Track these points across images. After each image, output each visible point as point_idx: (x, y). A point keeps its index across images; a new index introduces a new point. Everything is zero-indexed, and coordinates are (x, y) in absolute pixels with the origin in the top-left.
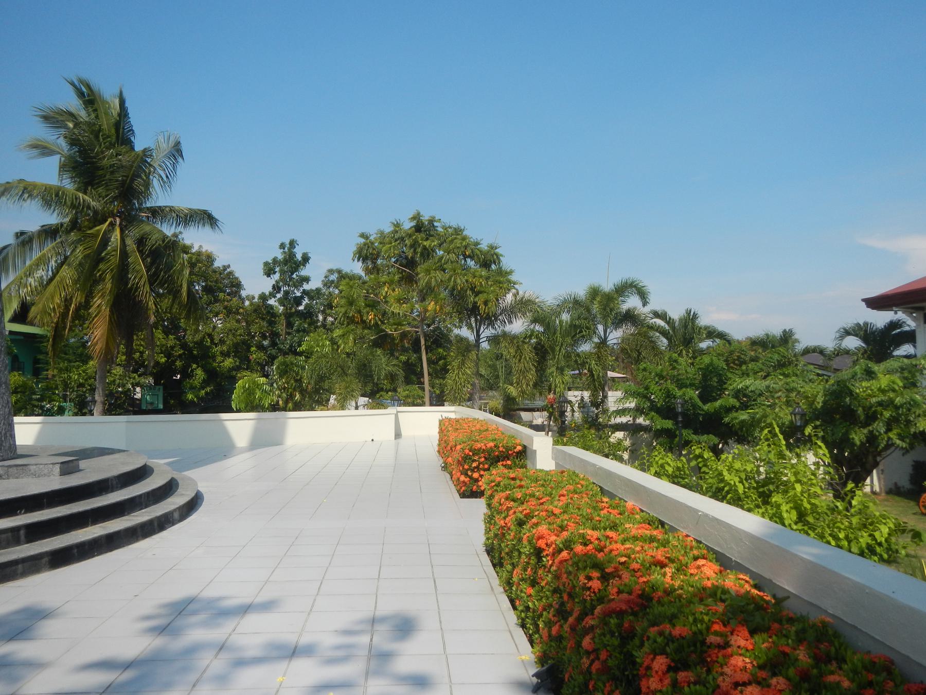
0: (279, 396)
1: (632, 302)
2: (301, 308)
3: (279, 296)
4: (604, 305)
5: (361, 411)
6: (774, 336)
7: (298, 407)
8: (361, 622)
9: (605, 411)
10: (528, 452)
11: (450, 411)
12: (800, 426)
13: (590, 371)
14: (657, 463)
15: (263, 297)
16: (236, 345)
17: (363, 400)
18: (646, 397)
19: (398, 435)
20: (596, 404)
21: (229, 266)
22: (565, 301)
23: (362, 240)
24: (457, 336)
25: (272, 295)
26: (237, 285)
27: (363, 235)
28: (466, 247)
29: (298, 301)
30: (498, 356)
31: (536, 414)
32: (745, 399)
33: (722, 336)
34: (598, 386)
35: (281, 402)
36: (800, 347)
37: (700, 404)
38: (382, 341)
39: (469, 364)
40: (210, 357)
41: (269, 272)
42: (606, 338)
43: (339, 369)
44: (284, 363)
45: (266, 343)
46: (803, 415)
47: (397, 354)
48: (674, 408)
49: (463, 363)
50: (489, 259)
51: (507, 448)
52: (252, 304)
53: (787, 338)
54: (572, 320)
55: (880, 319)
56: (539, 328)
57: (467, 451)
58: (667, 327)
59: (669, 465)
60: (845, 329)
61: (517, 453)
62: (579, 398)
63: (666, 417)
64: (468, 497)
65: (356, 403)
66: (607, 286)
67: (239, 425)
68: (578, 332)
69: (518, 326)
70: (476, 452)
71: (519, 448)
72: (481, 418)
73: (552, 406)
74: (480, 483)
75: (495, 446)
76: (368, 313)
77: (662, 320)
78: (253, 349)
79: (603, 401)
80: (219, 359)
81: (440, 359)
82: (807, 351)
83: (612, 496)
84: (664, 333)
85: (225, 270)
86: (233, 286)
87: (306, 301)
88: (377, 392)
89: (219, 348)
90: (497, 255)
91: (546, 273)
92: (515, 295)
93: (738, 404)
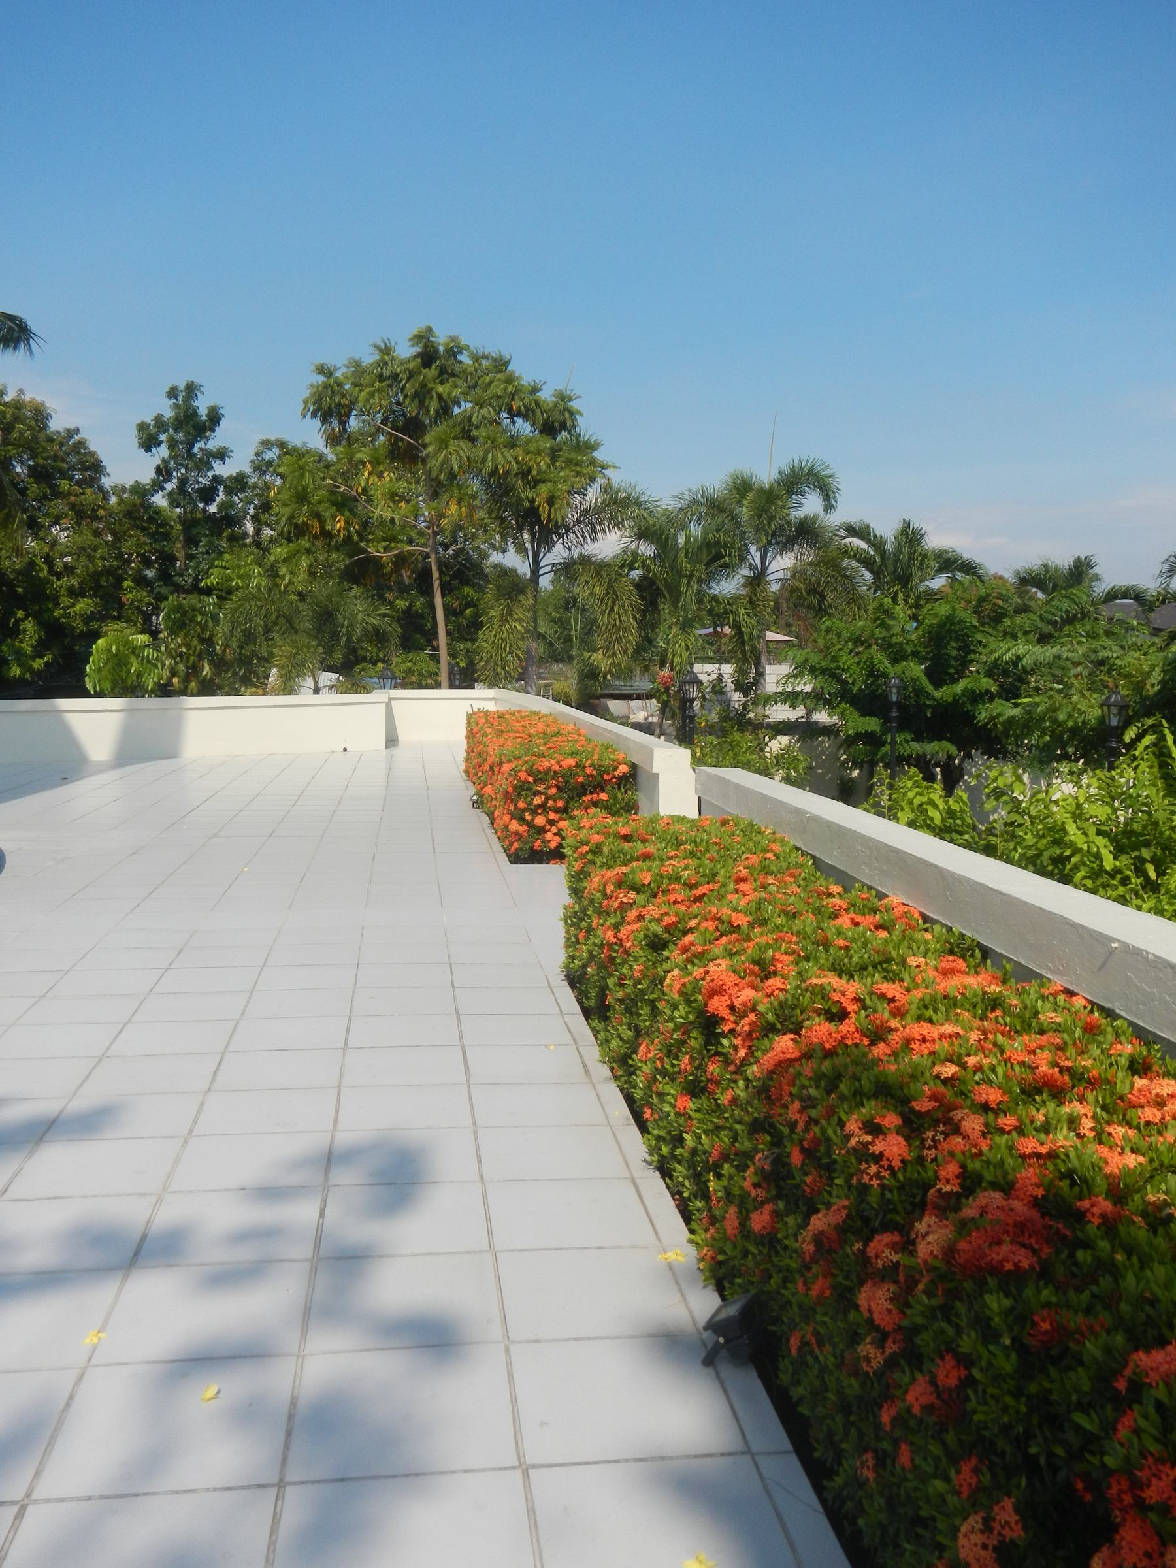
2: (213, 508)
3: (169, 486)
4: (761, 511)
5: (325, 697)
6: (1056, 569)
7: (207, 689)
8: (301, 1163)
10: (642, 779)
11: (485, 698)
12: (1117, 728)
13: (736, 626)
14: (911, 803)
15: (140, 491)
16: (95, 576)
17: (327, 678)
18: (832, 674)
19: (392, 741)
20: (740, 687)
21: (77, 431)
23: (321, 379)
24: (495, 566)
25: (157, 486)
26: (95, 467)
27: (321, 370)
28: (512, 396)
29: (208, 495)
30: (568, 603)
32: (1012, 681)
33: (968, 567)
34: (747, 656)
35: (175, 680)
36: (1101, 588)
37: (930, 688)
38: (362, 572)
39: (519, 613)
40: (48, 599)
41: (148, 442)
42: (764, 569)
43: (282, 621)
44: (179, 608)
45: (150, 574)
46: (1123, 708)
47: (389, 596)
48: (886, 697)
49: (510, 612)
50: (555, 422)
51: (601, 770)
52: (121, 501)
53: (1080, 571)
54: (705, 533)
56: (647, 549)
57: (523, 775)
59: (936, 806)
61: (620, 778)
62: (714, 676)
63: (865, 712)
64: (525, 861)
65: (316, 683)
66: (766, 475)
67: (94, 722)
68: (717, 556)
69: (609, 544)
70: (540, 776)
71: (623, 769)
72: (545, 711)
73: (667, 690)
74: (549, 836)
75: (577, 765)
78: (127, 584)
79: (756, 683)
80: (65, 601)
81: (468, 606)
82: (1112, 596)
83: (846, 881)
84: (867, 563)
86: (85, 469)
87: (221, 496)
88: (354, 663)
89: (64, 581)
90: (571, 413)
91: (662, 447)
92: (606, 489)
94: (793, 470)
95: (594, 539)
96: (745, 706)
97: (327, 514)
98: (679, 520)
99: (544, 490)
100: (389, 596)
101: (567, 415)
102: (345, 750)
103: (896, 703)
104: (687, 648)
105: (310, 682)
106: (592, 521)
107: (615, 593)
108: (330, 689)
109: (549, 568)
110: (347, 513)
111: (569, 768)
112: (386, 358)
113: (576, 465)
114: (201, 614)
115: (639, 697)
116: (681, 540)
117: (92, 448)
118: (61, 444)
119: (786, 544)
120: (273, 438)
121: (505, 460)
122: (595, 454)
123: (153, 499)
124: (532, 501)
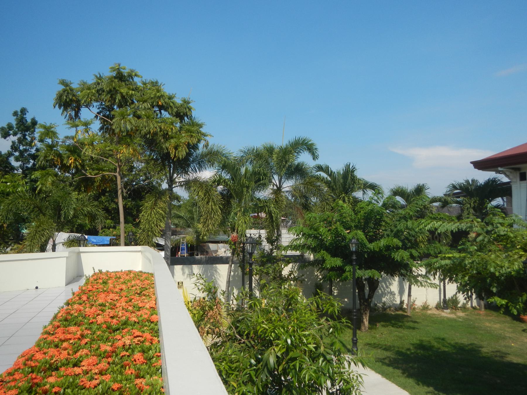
1: (304, 158)
9: (278, 248)
13: (270, 213)
28: (159, 98)
30: (194, 205)
31: (220, 245)
39: (161, 204)
42: (280, 186)
49: (155, 204)
50: (182, 113)
54: (254, 168)
55: (483, 177)
56: (226, 176)
58: (329, 179)
60: (453, 185)
62: (257, 236)
63: (334, 255)
68: (260, 179)
76: (68, 157)
77: (324, 172)
82: (434, 200)
91: (233, 129)
92: (206, 146)
93: (400, 244)
96: (272, 250)
98: (241, 161)
101: (187, 110)
102: (37, 288)
107: (209, 195)
113: (191, 132)
116: (243, 170)
120: (70, 135)
121: (153, 127)
122: (201, 129)
124: (167, 149)
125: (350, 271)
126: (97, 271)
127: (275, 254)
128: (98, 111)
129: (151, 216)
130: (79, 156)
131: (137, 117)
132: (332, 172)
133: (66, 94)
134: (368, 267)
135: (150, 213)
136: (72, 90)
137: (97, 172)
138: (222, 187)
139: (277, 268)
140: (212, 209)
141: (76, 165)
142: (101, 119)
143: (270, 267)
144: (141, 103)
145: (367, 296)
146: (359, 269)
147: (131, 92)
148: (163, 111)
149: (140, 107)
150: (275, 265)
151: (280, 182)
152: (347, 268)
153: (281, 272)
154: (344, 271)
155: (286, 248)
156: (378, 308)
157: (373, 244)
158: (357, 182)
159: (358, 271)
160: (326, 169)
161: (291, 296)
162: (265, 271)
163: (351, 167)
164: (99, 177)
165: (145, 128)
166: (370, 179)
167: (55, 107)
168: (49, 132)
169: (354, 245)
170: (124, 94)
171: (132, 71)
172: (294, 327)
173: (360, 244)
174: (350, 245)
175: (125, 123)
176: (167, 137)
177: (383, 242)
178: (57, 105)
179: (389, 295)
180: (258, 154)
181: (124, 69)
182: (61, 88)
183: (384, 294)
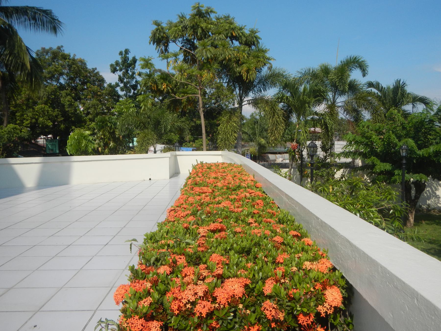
0: (99, 144)
1: (355, 75)
5: (159, 154)
9: (332, 155)
17: (159, 147)
18: (366, 145)
22: (305, 75)
23: (155, 27)
26: (102, 80)
30: (255, 123)
31: (278, 156)
35: (100, 149)
42: (334, 101)
43: (142, 124)
47: (194, 120)
49: (230, 118)
50: (251, 41)
58: (379, 94)
63: (383, 160)
65: (155, 149)
71: (334, 297)
73: (294, 150)
76: (162, 84)
77: (375, 88)
79: (331, 148)
80: (88, 123)
85: (94, 71)
92: (270, 68)
94: (347, 61)
95: (265, 90)
96: (325, 157)
97: (159, 83)
98: (299, 81)
99: (245, 67)
100: (194, 120)
101: (255, 39)
102: (150, 179)
103: (405, 157)
104: (306, 132)
105: (152, 148)
106: (266, 82)
107: (274, 110)
108: (161, 151)
109: (246, 103)
110: (167, 82)
111: (233, 302)
112: (182, 20)
114: (110, 123)
115: (280, 153)
116: (302, 88)
117: (100, 74)
118: (90, 73)
119: (343, 93)
121: (228, 54)
123: (116, 89)
124: (240, 73)
125: (399, 174)
126: (199, 162)
127: (329, 160)
128: (181, 45)
129: (227, 129)
130: (170, 82)
131: (214, 47)
132: (382, 87)
133: (158, 32)
134: (416, 172)
135: (224, 126)
136: (162, 28)
137: (183, 94)
138: (282, 104)
139: (331, 172)
140: (277, 121)
141: (168, 90)
142: (185, 51)
143: (324, 171)
144: (217, 35)
145: (413, 198)
146: (408, 173)
147: (209, 26)
148: (234, 41)
149: (216, 38)
150: (329, 170)
151: (334, 98)
152: (396, 172)
153: (333, 175)
154: (393, 175)
155: (339, 155)
156: (423, 209)
157: (422, 151)
158: (406, 96)
159: (406, 175)
160: (377, 86)
161: (354, 184)
162: (320, 174)
163: (401, 83)
164: (184, 99)
165: (222, 55)
166: (420, 93)
167: (150, 44)
168: (147, 64)
169: (404, 151)
170: (204, 28)
171: (209, 8)
172: (362, 204)
173: (410, 151)
174: (401, 151)
175: (206, 52)
176: (238, 62)
177: (432, 149)
178: (152, 42)
179: (433, 198)
180: (314, 75)
181: (202, 7)
182: (155, 27)
183: (429, 198)
